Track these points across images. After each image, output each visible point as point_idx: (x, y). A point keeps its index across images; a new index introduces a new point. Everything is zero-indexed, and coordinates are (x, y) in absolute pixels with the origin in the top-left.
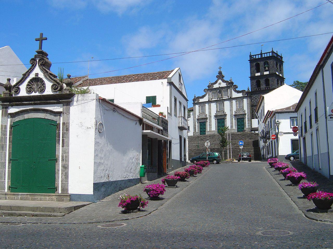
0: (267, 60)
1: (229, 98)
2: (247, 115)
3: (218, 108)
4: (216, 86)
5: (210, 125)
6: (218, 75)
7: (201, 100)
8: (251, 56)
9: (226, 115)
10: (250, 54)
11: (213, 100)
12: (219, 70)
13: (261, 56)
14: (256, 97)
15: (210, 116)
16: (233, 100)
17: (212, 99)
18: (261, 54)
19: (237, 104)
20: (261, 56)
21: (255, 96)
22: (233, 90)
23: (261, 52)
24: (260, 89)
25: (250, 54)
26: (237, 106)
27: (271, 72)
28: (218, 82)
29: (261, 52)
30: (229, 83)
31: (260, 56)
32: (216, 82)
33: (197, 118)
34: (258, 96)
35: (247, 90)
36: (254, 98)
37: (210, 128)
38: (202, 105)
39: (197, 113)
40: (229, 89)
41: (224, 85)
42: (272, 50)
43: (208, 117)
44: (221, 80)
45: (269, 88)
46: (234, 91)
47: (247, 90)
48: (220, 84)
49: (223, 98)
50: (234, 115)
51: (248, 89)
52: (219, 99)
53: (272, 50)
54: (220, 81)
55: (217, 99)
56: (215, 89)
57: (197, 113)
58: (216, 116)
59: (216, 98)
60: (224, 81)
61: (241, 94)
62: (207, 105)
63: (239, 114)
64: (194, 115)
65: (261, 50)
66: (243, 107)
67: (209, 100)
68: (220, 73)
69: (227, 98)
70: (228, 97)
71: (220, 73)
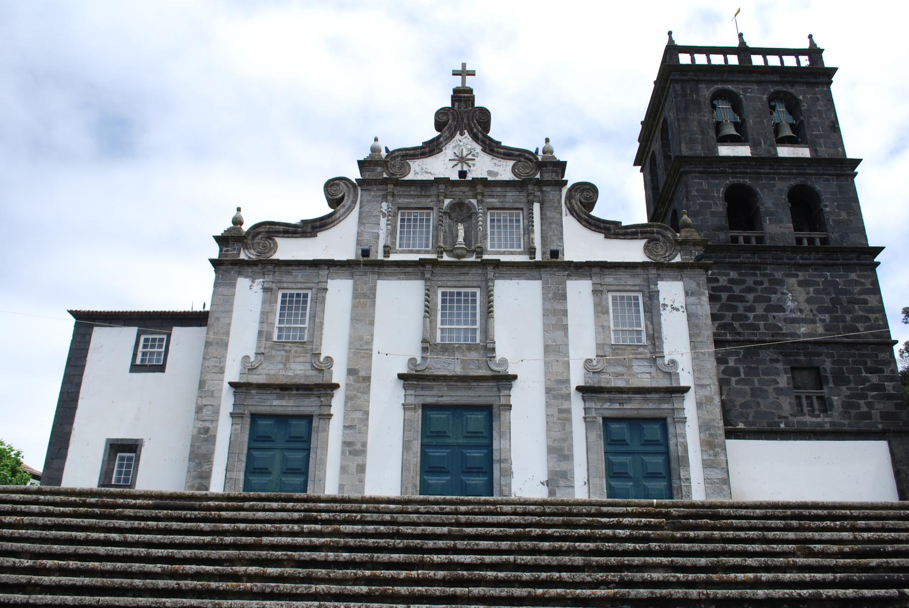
0: (792, 84)
1: (538, 257)
2: (689, 404)
3: (439, 325)
8: (672, 50)
9: (506, 380)
10: (671, 40)
12: (457, 82)
14: (737, 290)
17: (387, 252)
19: (600, 310)
21: (731, 281)
22: (572, 211)
24: (760, 239)
25: (671, 40)
26: (601, 328)
27: (824, 152)
28: (449, 151)
30: (541, 166)
32: (431, 149)
33: (233, 373)
34: (750, 281)
36: (724, 295)
37: (353, 468)
38: (295, 283)
40: (536, 207)
43: (338, 375)
44: (475, 138)
45: (824, 241)
46: (579, 219)
49: (485, 257)
50: (579, 389)
52: (446, 258)
54: (464, 142)
55: (434, 256)
56: (423, 185)
60: (493, 148)
61: (640, 244)
63: (621, 383)
67: (365, 253)
68: (462, 96)
69: (525, 258)
70: (531, 251)
71: (462, 96)
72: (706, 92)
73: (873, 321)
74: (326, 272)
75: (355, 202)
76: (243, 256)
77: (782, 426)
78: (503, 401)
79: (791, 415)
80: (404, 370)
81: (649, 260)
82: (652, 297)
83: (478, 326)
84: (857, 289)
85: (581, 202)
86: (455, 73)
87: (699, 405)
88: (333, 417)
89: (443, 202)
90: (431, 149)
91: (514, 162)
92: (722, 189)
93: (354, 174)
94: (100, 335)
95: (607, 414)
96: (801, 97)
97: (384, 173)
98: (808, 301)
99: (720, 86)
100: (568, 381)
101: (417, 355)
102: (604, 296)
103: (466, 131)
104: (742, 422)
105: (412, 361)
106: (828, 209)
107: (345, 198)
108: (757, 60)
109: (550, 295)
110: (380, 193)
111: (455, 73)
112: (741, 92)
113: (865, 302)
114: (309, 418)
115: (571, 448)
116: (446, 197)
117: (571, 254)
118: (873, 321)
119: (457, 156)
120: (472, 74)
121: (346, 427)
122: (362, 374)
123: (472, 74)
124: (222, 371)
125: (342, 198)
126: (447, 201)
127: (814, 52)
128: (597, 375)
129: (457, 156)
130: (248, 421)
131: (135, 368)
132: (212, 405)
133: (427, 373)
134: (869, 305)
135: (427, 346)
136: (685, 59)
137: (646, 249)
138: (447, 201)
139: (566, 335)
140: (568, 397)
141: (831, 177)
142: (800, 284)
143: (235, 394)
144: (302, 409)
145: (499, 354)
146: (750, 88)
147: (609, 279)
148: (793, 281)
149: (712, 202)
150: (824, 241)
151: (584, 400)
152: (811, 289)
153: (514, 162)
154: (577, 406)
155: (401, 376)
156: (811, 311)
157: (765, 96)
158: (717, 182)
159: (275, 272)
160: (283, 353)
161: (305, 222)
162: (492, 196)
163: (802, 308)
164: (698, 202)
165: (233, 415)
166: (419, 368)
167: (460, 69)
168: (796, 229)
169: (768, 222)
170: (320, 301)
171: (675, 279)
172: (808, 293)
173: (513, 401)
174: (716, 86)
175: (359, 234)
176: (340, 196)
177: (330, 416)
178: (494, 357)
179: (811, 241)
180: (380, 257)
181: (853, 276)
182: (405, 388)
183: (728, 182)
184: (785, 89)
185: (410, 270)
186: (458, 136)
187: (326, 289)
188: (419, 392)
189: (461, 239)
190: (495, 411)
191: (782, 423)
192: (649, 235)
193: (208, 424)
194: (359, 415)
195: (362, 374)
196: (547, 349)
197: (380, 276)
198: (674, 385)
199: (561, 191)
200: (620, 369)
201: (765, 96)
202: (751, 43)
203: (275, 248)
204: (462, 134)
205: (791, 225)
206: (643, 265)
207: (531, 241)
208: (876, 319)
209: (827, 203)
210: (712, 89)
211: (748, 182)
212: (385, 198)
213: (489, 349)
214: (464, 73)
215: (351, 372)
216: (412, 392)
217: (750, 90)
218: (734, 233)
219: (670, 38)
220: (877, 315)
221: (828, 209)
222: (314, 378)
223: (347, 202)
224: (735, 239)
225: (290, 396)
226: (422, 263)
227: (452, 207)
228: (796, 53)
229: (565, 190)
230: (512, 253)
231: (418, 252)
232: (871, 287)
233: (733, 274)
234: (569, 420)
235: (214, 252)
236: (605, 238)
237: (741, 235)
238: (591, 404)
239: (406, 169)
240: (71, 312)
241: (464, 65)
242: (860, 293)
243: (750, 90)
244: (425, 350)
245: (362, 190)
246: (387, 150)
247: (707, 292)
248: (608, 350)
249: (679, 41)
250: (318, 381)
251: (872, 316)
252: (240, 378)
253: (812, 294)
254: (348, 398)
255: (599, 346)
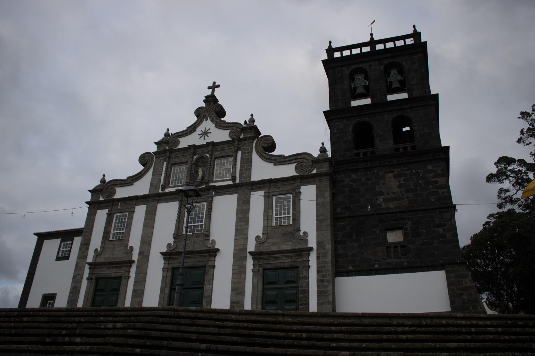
1: (237, 181)
4: (184, 143)
5: (139, 293)
6: (203, 105)
7: (121, 193)
8: (330, 51)
9: (214, 252)
11: (167, 190)
12: (209, 92)
13: (373, 48)
15: (145, 255)
16: (252, 190)
18: (372, 43)
19: (268, 208)
20: (373, 48)
22: (257, 152)
23: (372, 38)
28: (200, 129)
29: (372, 38)
31: (366, 49)
35: (316, 153)
36: (347, 189)
39: (96, 242)
40: (240, 153)
41: (222, 136)
42: (415, 30)
43: (135, 257)
44: (212, 121)
47: (316, 153)
48: (205, 134)
49: (211, 184)
51: (323, 150)
53: (415, 30)
54: (208, 124)
57: (96, 242)
58: (167, 255)
59: (182, 186)
61: (293, 166)
62: (140, 211)
63: (274, 248)
64: (85, 245)
65: (371, 34)
66: (296, 218)
68: (211, 100)
69: (230, 183)
70: (234, 179)
71: (211, 100)
72: (347, 71)
73: (441, 194)
74: (134, 203)
75: (151, 164)
76: (101, 199)
77: (376, 266)
78: (210, 263)
79: (383, 259)
80: (165, 250)
81: (298, 175)
82: (297, 195)
83: (203, 223)
84: (431, 175)
85: (263, 147)
86: (209, 88)
87: (318, 257)
88: (130, 278)
89: (193, 158)
90: (192, 129)
91: (230, 130)
92: (351, 126)
93: (153, 149)
94: (47, 244)
95: (265, 266)
96: (404, 64)
97: (167, 147)
98: (399, 186)
99: (355, 66)
100: (246, 249)
101: (171, 241)
102: (270, 199)
103: (208, 118)
104: (351, 266)
105: (169, 245)
106: (416, 128)
107: (148, 163)
108: (380, 47)
109: (241, 202)
110: (164, 158)
111: (209, 88)
112: (368, 67)
113: (436, 182)
114: (120, 278)
115: (244, 287)
116: (194, 155)
117: (256, 177)
118: (441, 194)
119: (202, 132)
120: (218, 86)
121: (135, 282)
122: (145, 254)
123: (218, 86)
124: (86, 257)
125: (146, 163)
126: (195, 157)
127: (416, 35)
128: (261, 245)
129: (202, 132)
130: (94, 281)
131: (58, 259)
132: (79, 275)
133: (176, 251)
134: (439, 184)
135: (177, 236)
136: (337, 55)
137: (296, 168)
138: (195, 157)
139: (247, 224)
140: (245, 259)
141: (420, 108)
142: (395, 176)
143: (90, 268)
144: (117, 274)
145: (211, 238)
146: (374, 64)
147: (273, 189)
148: (390, 175)
149: (345, 135)
150: (413, 148)
151: (253, 259)
152: (402, 179)
153: (230, 130)
154: (250, 263)
155: (162, 253)
156: (401, 192)
157: (382, 67)
158: (349, 122)
159: (113, 205)
160: (113, 246)
161: (128, 178)
162: (217, 151)
163: (395, 191)
164: (337, 136)
165: (88, 279)
166: (172, 248)
167: (211, 85)
168: (395, 143)
169: (378, 141)
170: (131, 218)
171: (311, 183)
172: (399, 182)
173: (217, 263)
174: (353, 67)
175: (152, 181)
176: (146, 162)
177: (129, 277)
178: (209, 240)
179: (405, 148)
180: (160, 191)
181: (430, 167)
182: (164, 259)
183: (355, 121)
184: (394, 61)
185: (173, 196)
186: (205, 121)
187: (134, 212)
188: (171, 261)
189: (200, 177)
190: (207, 269)
191: (376, 264)
192: (298, 160)
193: (77, 284)
194: (142, 275)
195: (145, 254)
196: (237, 231)
197: (159, 201)
198: (304, 247)
199: (253, 142)
200: (274, 240)
201: (382, 67)
202: (376, 38)
203: (114, 193)
204: (206, 120)
205: (392, 141)
206: (293, 178)
207: (234, 172)
208: (443, 193)
209: (416, 124)
210: (350, 69)
211: (367, 119)
212: (165, 160)
213: (207, 235)
214: (214, 86)
215: (140, 253)
216: (167, 262)
217: (373, 65)
218: (357, 151)
219: (330, 45)
220: (444, 190)
221: (416, 128)
222: (125, 258)
223: (148, 165)
224: (357, 155)
225: (113, 267)
226: (178, 192)
227: (198, 160)
228: (404, 38)
229: (255, 142)
230: (224, 181)
231: (175, 187)
232: (441, 172)
233: (354, 176)
234: (244, 272)
235: (88, 197)
236: (274, 165)
237: (361, 152)
238: (257, 262)
239: (178, 143)
240: (35, 234)
241: (214, 83)
242: (433, 177)
243: (373, 65)
244: (174, 238)
245: (156, 157)
246: (171, 133)
247: (329, 189)
248: (269, 229)
249: (334, 46)
250: (126, 259)
251: (440, 191)
252: (93, 260)
253: (402, 182)
254: (138, 267)
255: (266, 228)
